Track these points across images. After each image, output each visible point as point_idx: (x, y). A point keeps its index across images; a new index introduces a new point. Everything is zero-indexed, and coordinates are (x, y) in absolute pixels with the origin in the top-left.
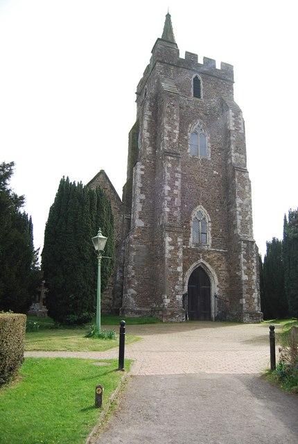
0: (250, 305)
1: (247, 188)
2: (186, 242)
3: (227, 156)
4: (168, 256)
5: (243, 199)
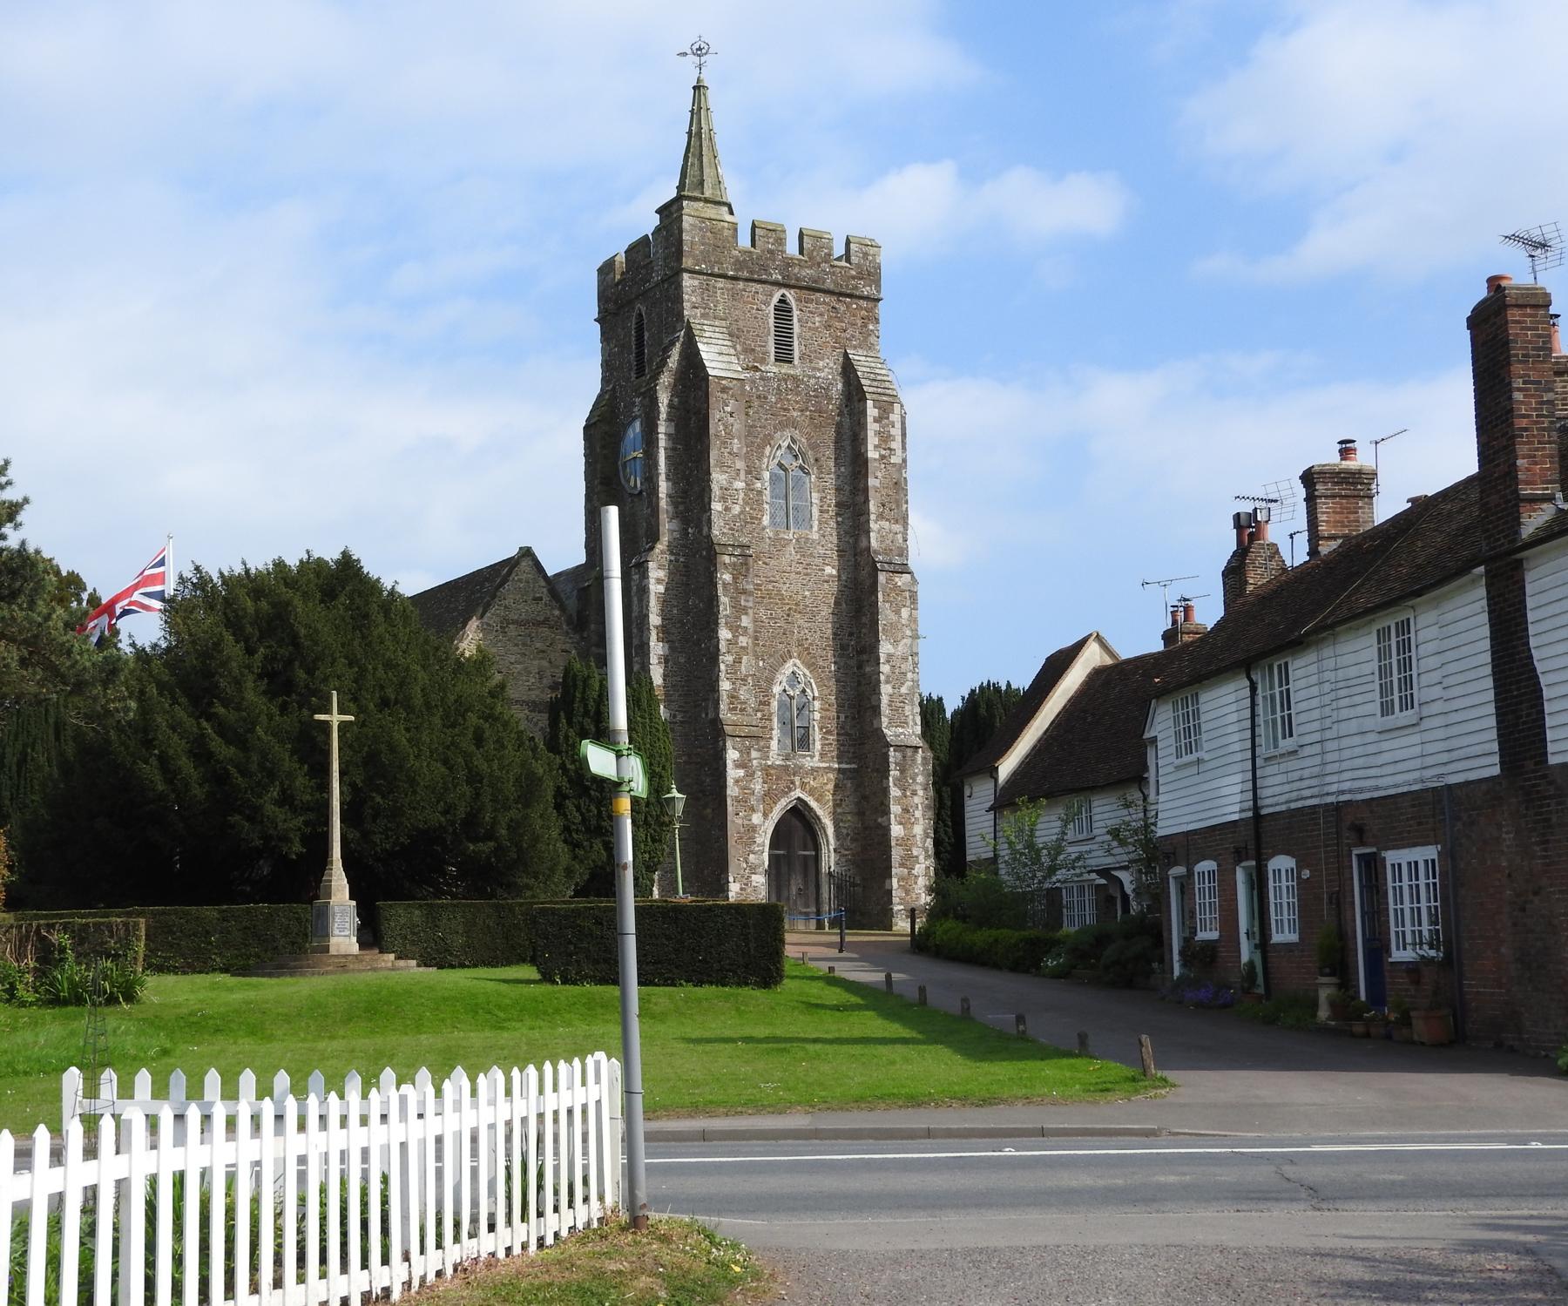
0: (907, 892)
1: (905, 612)
4: (732, 791)
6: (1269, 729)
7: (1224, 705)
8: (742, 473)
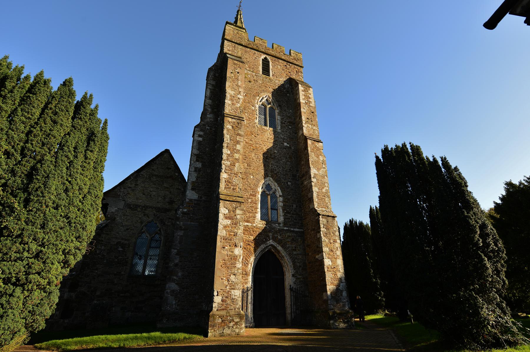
4: (221, 232)
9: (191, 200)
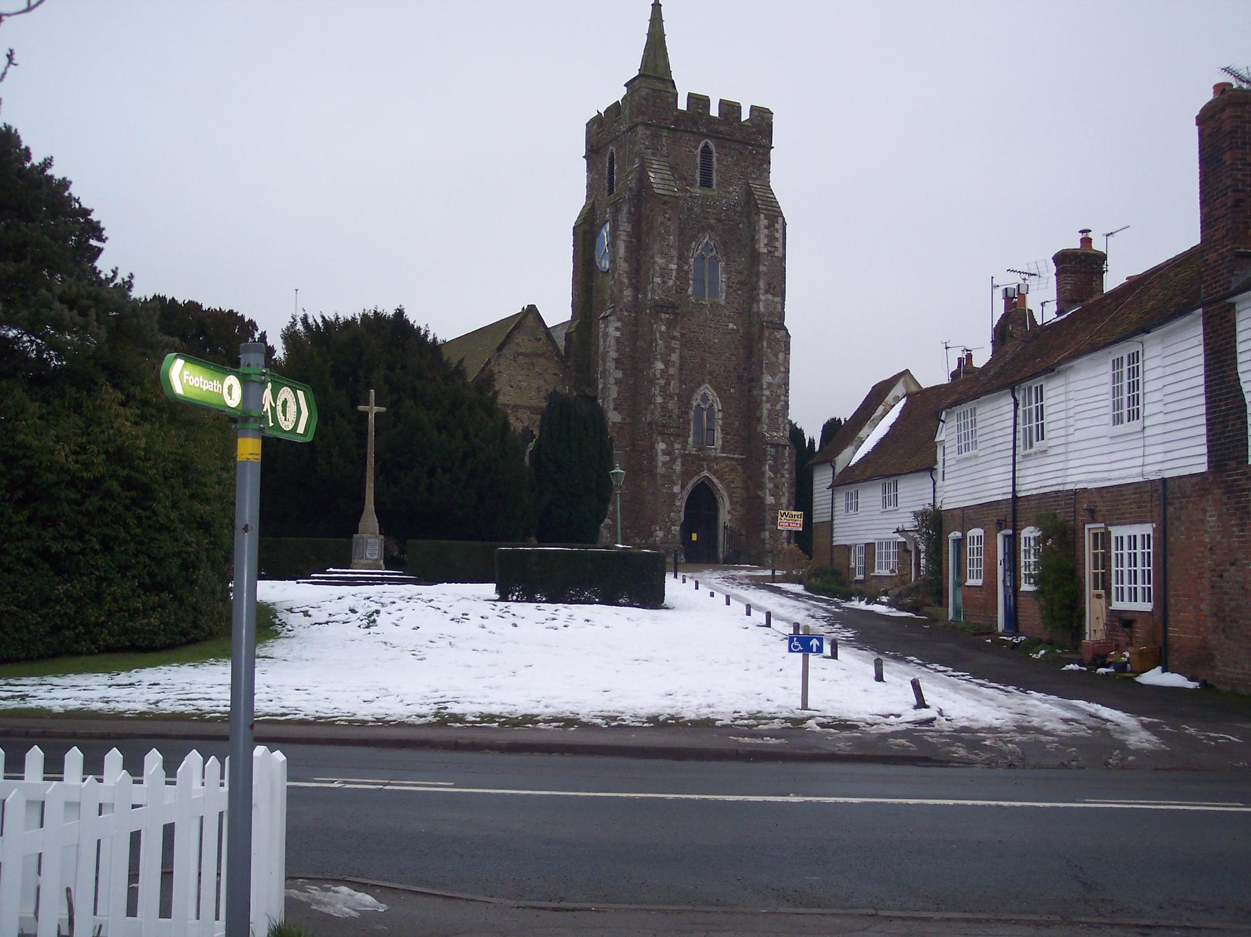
0: (775, 541)
1: (781, 356)
2: (684, 448)
3: (752, 298)
4: (661, 470)
5: (773, 376)
6: (1030, 434)
7: (996, 415)
8: (675, 260)
9: (614, 423)
